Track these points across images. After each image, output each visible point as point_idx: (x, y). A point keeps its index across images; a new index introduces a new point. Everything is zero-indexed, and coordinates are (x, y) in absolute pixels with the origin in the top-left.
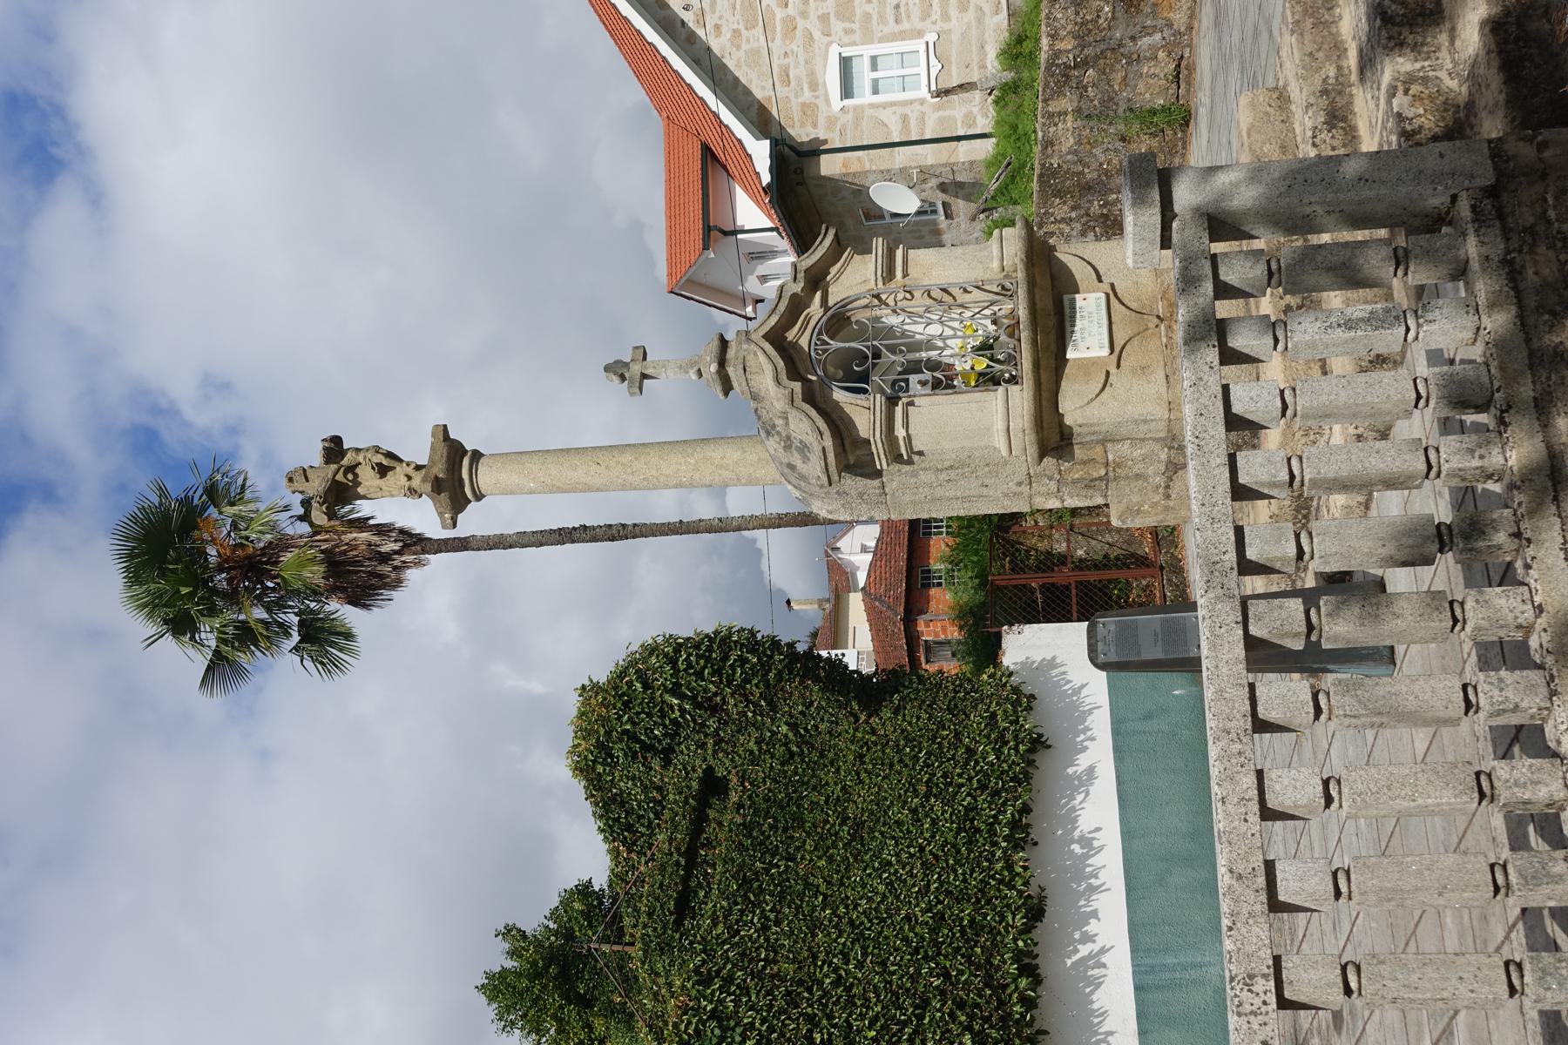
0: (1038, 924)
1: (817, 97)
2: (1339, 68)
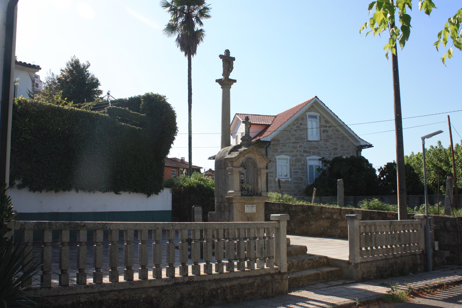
1: (279, 153)
2: (294, 255)
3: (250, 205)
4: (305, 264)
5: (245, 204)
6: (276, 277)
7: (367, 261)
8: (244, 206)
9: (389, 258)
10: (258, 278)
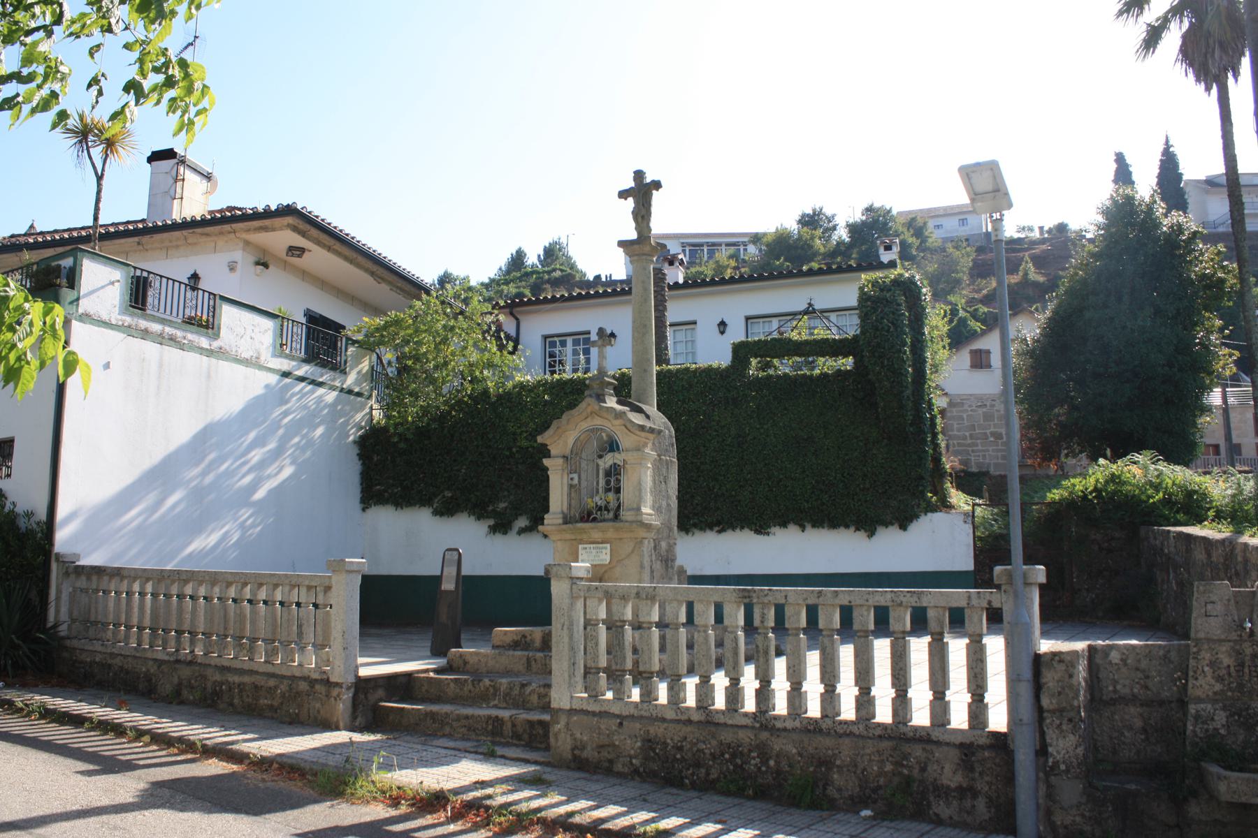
3: (592, 546)
4: (530, 694)
5: (581, 541)
6: (318, 687)
7: (605, 712)
9: (730, 722)
10: (285, 682)
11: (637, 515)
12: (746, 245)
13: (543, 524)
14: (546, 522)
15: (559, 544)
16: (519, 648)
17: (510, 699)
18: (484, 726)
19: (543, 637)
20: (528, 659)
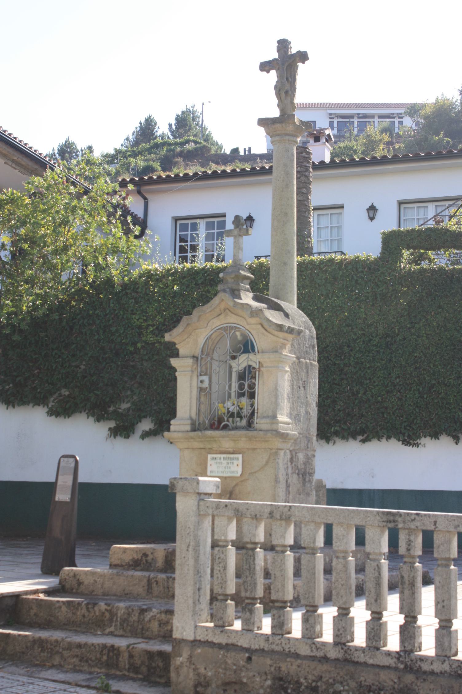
0: (401, 442)
3: (222, 456)
4: (150, 621)
5: (211, 451)
7: (233, 645)
8: (207, 458)
9: (371, 661)
11: (272, 423)
12: (402, 118)
13: (168, 430)
14: (172, 428)
15: (186, 452)
16: (139, 568)
17: (128, 625)
18: (98, 656)
19: (166, 557)
20: (149, 580)
